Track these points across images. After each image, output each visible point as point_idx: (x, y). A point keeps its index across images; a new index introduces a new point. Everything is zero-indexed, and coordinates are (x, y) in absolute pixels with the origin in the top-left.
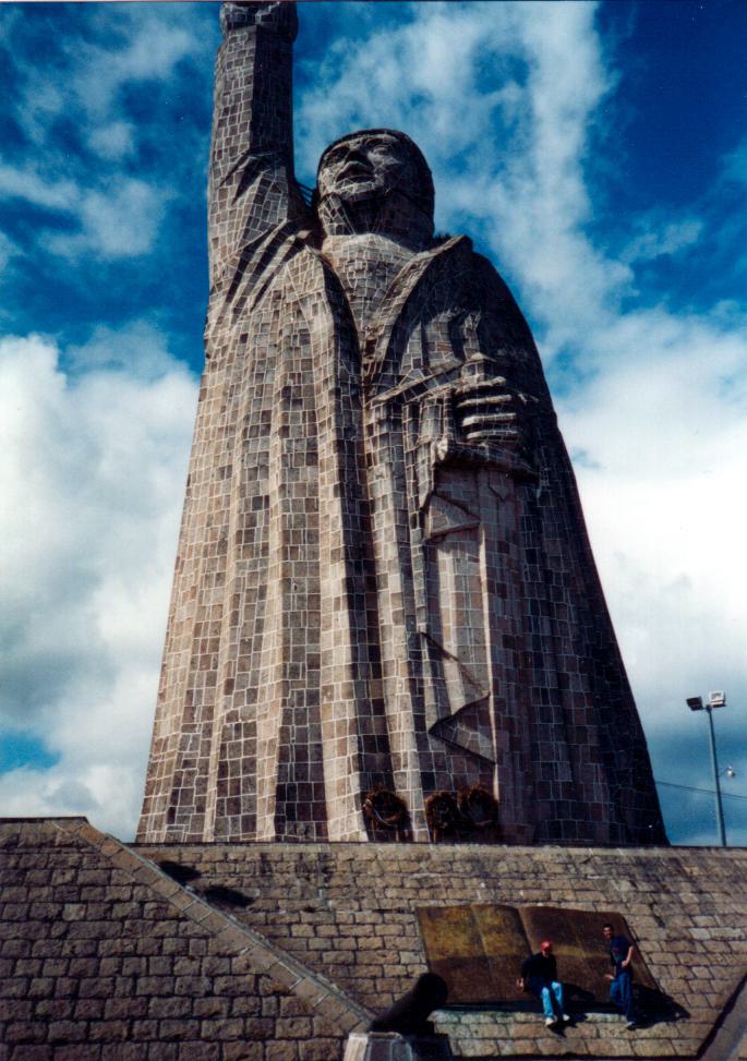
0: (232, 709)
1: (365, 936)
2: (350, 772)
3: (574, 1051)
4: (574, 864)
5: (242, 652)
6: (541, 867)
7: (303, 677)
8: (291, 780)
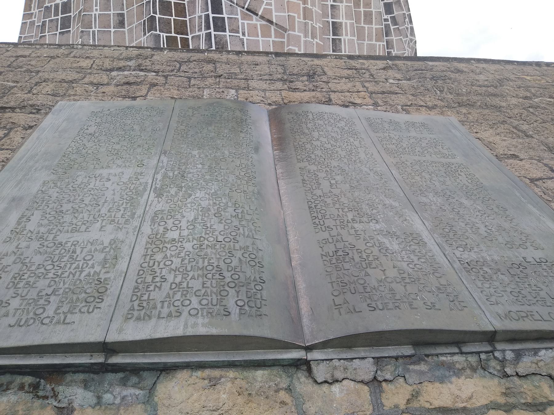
2: (145, 34)
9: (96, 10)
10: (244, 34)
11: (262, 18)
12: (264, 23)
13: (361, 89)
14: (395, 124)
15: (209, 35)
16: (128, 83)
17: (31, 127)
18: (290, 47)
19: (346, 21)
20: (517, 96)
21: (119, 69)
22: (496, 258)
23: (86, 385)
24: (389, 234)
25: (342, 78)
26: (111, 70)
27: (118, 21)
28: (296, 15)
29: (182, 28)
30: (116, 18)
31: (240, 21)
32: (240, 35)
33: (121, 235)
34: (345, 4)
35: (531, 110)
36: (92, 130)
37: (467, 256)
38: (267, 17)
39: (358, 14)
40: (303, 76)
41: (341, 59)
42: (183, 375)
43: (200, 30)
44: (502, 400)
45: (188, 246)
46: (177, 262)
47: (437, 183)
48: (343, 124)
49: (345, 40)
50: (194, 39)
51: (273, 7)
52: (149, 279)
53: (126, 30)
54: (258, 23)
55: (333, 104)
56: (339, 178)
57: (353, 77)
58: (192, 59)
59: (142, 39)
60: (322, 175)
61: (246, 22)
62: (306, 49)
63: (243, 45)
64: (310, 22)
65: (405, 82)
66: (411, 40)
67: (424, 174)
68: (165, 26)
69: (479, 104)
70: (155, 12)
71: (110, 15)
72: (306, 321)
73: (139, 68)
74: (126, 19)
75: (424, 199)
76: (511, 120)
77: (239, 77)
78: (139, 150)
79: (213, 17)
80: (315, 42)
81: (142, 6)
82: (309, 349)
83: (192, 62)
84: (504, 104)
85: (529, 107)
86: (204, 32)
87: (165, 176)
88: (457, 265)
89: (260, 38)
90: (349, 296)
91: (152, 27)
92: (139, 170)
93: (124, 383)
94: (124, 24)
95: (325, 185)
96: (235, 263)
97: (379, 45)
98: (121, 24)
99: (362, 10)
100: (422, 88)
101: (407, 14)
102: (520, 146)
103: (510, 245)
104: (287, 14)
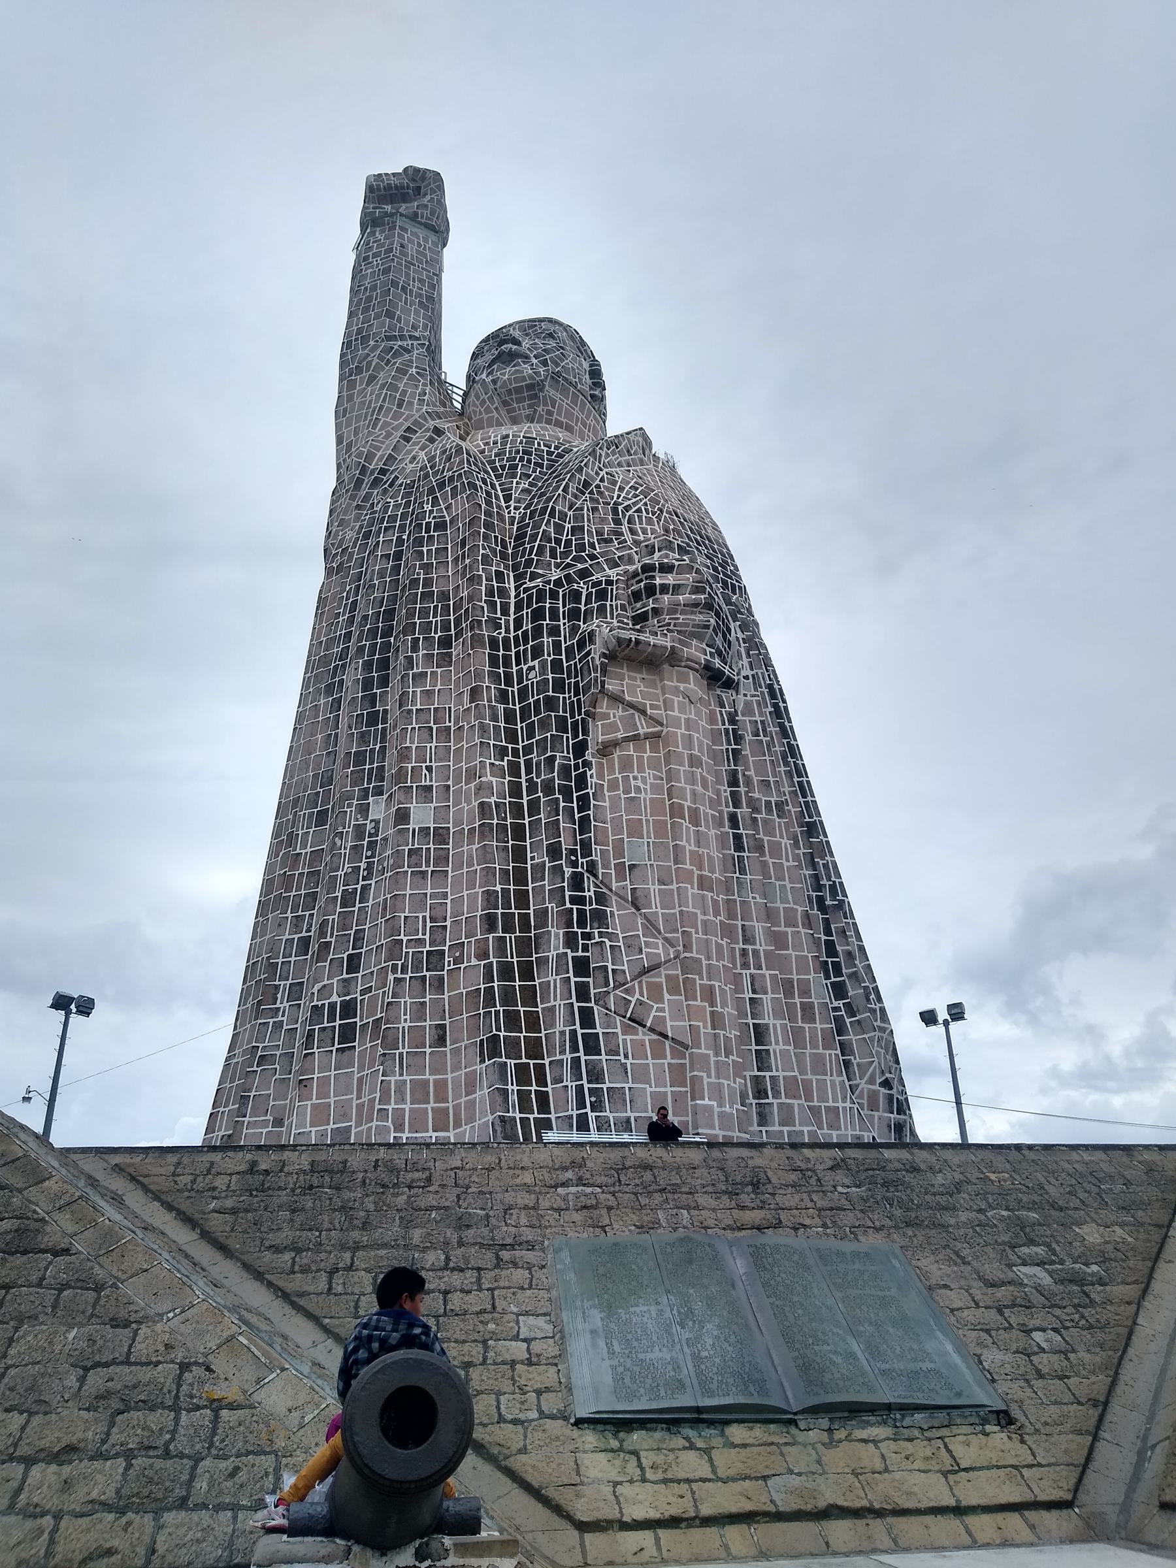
0: (326, 982)
1: (462, 1291)
2: (482, 1061)
3: (841, 1502)
4: (814, 1171)
5: (343, 906)
6: (762, 1175)
7: (424, 934)
8: (401, 1075)
9: (405, 1020)
10: (626, 1057)
11: (652, 1030)
12: (655, 1037)
13: (810, 1205)
14: (840, 1254)
15: (576, 1062)
16: (585, 1207)
17: (543, 1267)
18: (695, 1073)
19: (775, 1022)
20: (970, 1209)
21: (563, 1185)
22: (902, 1367)
23: (692, 1428)
24: (835, 1352)
25: (787, 1186)
26: (556, 1187)
27: (436, 1037)
28: (701, 1024)
29: (535, 1049)
30: (433, 1031)
31: (621, 1037)
32: (622, 1057)
33: (674, 1354)
34: (770, 995)
35: (978, 1229)
36: (601, 1270)
37: (884, 1366)
38: (658, 1029)
40: (748, 1185)
41: (783, 1148)
42: (735, 1425)
43: (563, 1052)
44: (893, 1436)
45: (717, 1360)
46: (715, 1370)
47: (872, 1315)
48: (796, 1258)
49: (775, 1052)
50: (554, 1066)
51: (667, 1014)
52: (704, 1378)
53: (448, 1049)
54: (647, 1038)
55: (783, 1227)
56: (800, 1312)
57: (800, 1186)
58: (628, 1164)
59: (478, 1067)
60: (787, 1309)
61: (628, 1038)
62: (718, 1073)
63: (627, 1072)
64: (722, 1032)
65: (853, 1189)
66: (883, 1030)
67: (863, 1307)
68: (513, 1048)
69: (926, 1223)
72: (791, 1401)
73: (580, 1182)
74: (448, 1034)
75: (861, 1328)
76: (956, 1243)
77: (683, 1190)
78: (649, 1290)
79: (582, 1034)
80: (730, 1062)
81: (477, 1017)
82: (795, 1414)
83: (627, 1169)
84: (952, 1221)
85: (978, 1225)
86: (568, 1056)
87: (679, 1313)
88: (876, 1371)
90: (814, 1387)
91: (494, 1052)
92: (659, 1307)
93: (708, 1427)
94: (445, 1041)
95: (791, 1317)
96: (747, 1370)
97: (830, 1055)
98: (441, 1040)
99: (797, 1000)
100: (872, 1200)
101: (871, 987)
102: (953, 1276)
103: (915, 1360)
104: (687, 1024)
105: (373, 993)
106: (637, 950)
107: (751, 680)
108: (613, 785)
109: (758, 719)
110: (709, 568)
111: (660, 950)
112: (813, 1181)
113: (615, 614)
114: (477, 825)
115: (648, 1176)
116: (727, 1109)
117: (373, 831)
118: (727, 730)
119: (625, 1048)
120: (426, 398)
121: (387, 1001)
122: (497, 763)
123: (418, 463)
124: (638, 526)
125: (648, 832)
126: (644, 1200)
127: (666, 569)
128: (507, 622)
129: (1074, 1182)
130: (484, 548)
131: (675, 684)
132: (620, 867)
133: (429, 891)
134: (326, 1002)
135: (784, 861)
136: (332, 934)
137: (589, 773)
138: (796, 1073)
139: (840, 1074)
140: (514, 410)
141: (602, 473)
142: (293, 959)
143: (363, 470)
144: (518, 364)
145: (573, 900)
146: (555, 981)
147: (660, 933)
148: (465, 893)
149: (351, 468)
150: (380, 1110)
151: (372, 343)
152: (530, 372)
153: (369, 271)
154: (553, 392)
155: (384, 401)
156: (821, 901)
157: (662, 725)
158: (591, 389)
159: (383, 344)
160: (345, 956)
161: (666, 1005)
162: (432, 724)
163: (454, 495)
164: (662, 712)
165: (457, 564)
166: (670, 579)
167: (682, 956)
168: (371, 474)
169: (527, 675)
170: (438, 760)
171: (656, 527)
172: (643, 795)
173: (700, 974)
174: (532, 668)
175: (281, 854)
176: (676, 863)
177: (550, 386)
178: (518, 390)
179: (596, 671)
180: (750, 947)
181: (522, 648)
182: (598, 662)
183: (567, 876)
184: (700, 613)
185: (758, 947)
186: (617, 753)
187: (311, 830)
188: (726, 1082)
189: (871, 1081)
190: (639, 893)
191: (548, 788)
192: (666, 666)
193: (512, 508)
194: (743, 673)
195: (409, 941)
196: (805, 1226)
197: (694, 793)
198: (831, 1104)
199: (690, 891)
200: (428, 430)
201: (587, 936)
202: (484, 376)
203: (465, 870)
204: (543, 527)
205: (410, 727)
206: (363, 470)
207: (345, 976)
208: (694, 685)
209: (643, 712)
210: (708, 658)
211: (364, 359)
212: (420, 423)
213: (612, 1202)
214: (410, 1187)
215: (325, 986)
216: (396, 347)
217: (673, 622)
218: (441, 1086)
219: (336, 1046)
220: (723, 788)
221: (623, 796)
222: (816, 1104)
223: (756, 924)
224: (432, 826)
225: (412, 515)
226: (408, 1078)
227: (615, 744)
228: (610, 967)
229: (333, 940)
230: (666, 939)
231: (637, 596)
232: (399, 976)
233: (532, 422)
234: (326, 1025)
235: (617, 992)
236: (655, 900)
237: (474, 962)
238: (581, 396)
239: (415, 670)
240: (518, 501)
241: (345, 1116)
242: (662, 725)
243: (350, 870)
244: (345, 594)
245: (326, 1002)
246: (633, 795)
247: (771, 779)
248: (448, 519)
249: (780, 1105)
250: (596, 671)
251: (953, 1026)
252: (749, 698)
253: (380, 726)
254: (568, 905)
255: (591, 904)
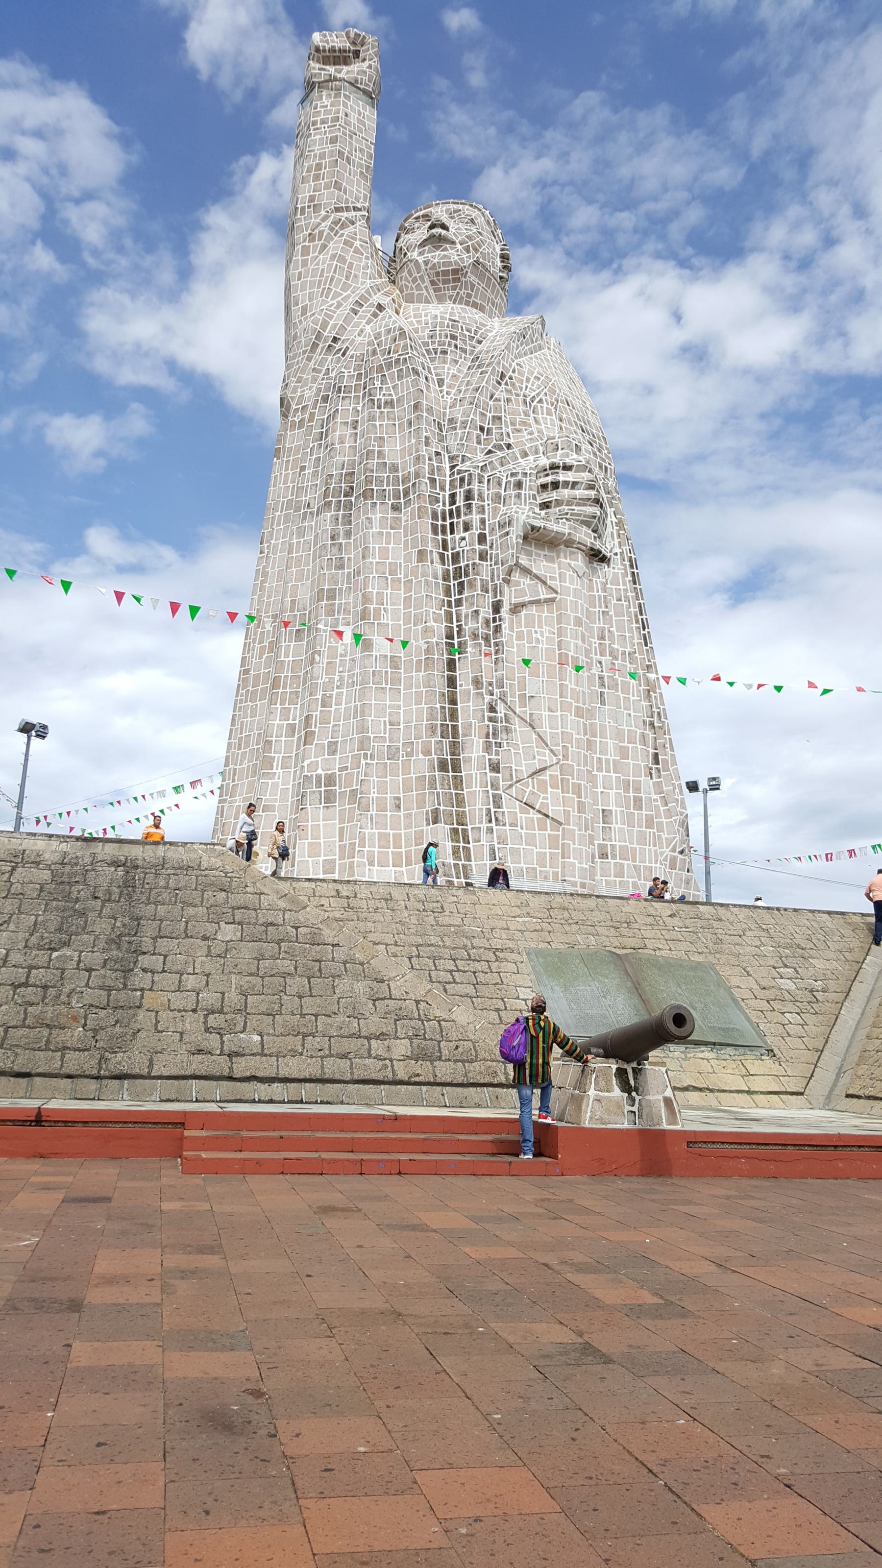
0: (313, 759)
7: (385, 733)
10: (522, 828)
11: (539, 812)
12: (540, 816)
31: (519, 815)
32: (519, 828)
34: (614, 791)
39: (627, 799)
43: (481, 822)
51: (549, 801)
54: (535, 817)
61: (524, 816)
70: (439, 804)
71: (386, 798)
89: (537, 832)
99: (631, 794)
105: (349, 771)
106: (532, 757)
107: (619, 556)
108: (520, 637)
109: (621, 587)
110: (590, 453)
111: (548, 758)
112: (661, 922)
113: (528, 502)
114: (423, 658)
115: (566, 914)
116: (584, 866)
117: (343, 652)
118: (600, 596)
119: (521, 823)
120: (369, 271)
121: (360, 778)
122: (437, 612)
123: (365, 336)
124: (540, 416)
125: (543, 673)
126: (567, 928)
127: (567, 468)
128: (444, 496)
129: (810, 933)
130: (427, 432)
131: (568, 561)
132: (522, 697)
133: (388, 703)
134: (314, 774)
135: (631, 696)
136: (316, 726)
137: (503, 626)
138: (627, 844)
139: (655, 846)
140: (439, 290)
141: (514, 364)
142: (283, 739)
143: (319, 336)
144: (445, 249)
145: (491, 719)
146: (476, 774)
147: (547, 745)
148: (414, 707)
149: (308, 333)
150: (359, 851)
151: (323, 213)
152: (456, 258)
153: (318, 137)
154: (473, 278)
155: (335, 272)
156: (652, 724)
157: (557, 592)
158: (500, 271)
159: (333, 215)
160: (326, 742)
161: (549, 796)
162: (387, 575)
163: (400, 377)
164: (558, 583)
165: (404, 440)
166: (570, 476)
167: (561, 762)
168: (325, 341)
169: (459, 543)
170: (393, 604)
171: (554, 418)
172: (540, 646)
173: (572, 775)
174: (463, 539)
175: (264, 657)
176: (561, 697)
177: (472, 273)
178: (445, 273)
179: (513, 548)
180: (604, 757)
181: (455, 520)
182: (514, 541)
183: (486, 701)
184: (590, 505)
185: (609, 757)
186: (524, 612)
187: (292, 644)
188: (584, 848)
189: (673, 850)
190: (534, 717)
191: (475, 636)
192: (562, 547)
193: (445, 393)
194: (614, 551)
195: (375, 737)
196: (659, 949)
197: (576, 645)
198: (647, 864)
199: (569, 718)
200: (372, 305)
201: (499, 745)
202: (415, 253)
203: (414, 690)
204: (472, 416)
205: (371, 576)
206: (319, 336)
207: (326, 756)
208: (579, 561)
209: (544, 583)
210: (592, 541)
211: (317, 227)
212: (366, 297)
213: (550, 929)
214: (433, 912)
215: (312, 762)
216: (343, 219)
217: (570, 512)
218: (397, 837)
219: (323, 804)
220: (594, 641)
221: (527, 645)
222: (637, 863)
223: (609, 741)
224: (389, 654)
225: (365, 388)
226: (377, 831)
227: (523, 605)
228: (514, 768)
229: (317, 730)
230: (551, 751)
231: (544, 487)
232: (369, 761)
233: (454, 303)
234: (314, 789)
235: (518, 785)
236: (546, 723)
237: (421, 756)
238: (493, 280)
239: (374, 530)
240: (449, 387)
241: (331, 852)
242: (557, 592)
243: (327, 680)
244: (309, 450)
245: (314, 774)
246: (534, 644)
247: (627, 634)
248: (394, 397)
249: (615, 864)
250: (513, 548)
251: (711, 794)
252: (616, 571)
253: (346, 571)
254: (487, 722)
255: (502, 722)
